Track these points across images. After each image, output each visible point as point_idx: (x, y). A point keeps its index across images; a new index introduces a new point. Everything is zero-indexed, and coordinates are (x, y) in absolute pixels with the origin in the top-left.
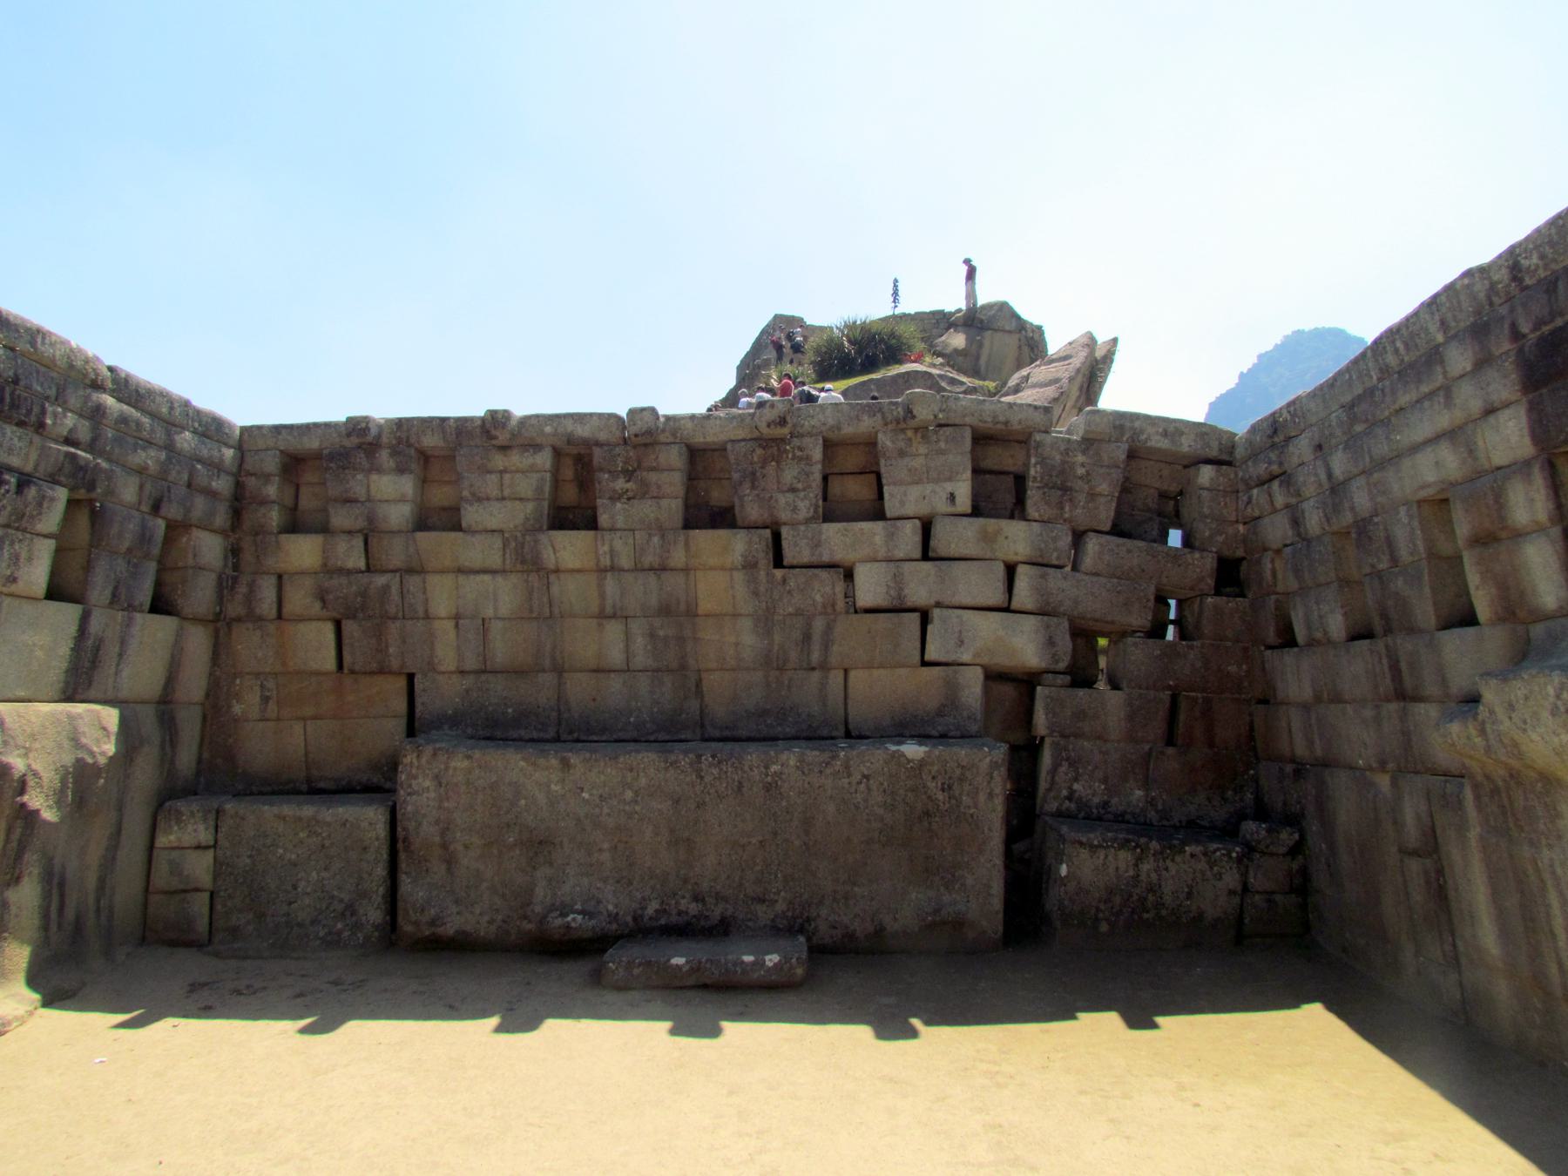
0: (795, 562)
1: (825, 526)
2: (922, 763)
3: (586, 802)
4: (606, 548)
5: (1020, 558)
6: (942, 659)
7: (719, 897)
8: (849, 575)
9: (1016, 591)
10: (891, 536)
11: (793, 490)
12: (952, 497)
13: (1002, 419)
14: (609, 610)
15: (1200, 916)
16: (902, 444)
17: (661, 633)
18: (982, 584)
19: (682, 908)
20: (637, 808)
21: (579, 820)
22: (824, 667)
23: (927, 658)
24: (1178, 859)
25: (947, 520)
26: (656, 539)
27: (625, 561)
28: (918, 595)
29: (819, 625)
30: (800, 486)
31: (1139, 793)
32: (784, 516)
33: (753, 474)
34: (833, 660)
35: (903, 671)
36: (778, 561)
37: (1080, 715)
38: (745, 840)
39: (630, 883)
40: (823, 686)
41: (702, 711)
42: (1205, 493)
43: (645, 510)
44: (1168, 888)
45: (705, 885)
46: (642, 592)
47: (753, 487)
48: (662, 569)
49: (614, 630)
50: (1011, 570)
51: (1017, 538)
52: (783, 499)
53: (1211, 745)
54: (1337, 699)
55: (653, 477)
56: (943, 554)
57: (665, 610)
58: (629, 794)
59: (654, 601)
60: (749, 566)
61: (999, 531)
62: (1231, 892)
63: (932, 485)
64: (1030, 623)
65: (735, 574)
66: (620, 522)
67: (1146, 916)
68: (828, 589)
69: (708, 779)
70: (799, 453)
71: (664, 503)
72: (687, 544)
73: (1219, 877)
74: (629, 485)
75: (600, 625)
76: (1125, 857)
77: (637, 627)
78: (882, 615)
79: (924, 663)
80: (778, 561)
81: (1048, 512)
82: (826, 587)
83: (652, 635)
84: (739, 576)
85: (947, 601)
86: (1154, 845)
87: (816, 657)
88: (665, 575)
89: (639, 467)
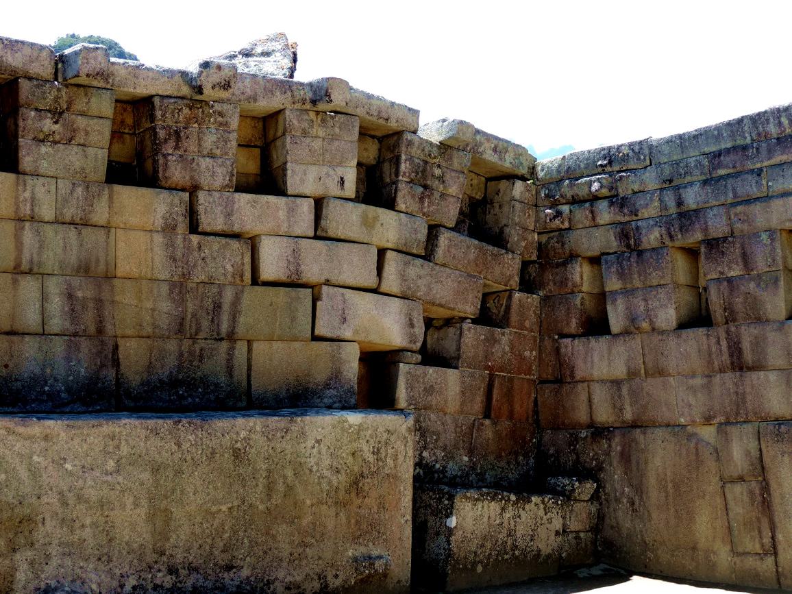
0: (209, 229)
1: (237, 195)
2: (361, 428)
3: (70, 474)
4: (27, 195)
5: (390, 245)
6: (329, 335)
7: (192, 569)
8: (253, 244)
9: (385, 274)
10: (291, 211)
11: (211, 156)
12: (342, 182)
13: (385, 115)
14: (25, 266)
15: (539, 554)
16: (305, 125)
17: (79, 294)
18: (357, 267)
19: (158, 582)
20: (120, 479)
21: (61, 493)
22: (231, 337)
23: (317, 332)
24: (527, 507)
25: (338, 202)
26: (79, 190)
27: (47, 213)
28: (312, 272)
29: (229, 295)
30: (218, 152)
31: (466, 459)
32: (204, 181)
33: (177, 133)
34: (241, 330)
35: (297, 345)
36: (194, 228)
37: (429, 390)
38: (214, 509)
39: (110, 561)
40: (230, 360)
41: (117, 379)
42: (518, 205)
43: (73, 157)
44: (521, 531)
45: (179, 557)
46: (58, 247)
47: (177, 147)
48: (81, 224)
49: (29, 287)
50: (382, 253)
51: (390, 227)
52: (205, 163)
53: (511, 416)
54: (661, 372)
55: (81, 122)
56: (331, 234)
57: (84, 269)
58: (111, 464)
59: (73, 259)
60: (169, 229)
61: (376, 218)
62: (557, 533)
63: (321, 168)
64: (396, 304)
65: (155, 236)
66: (44, 166)
67: (506, 557)
68: (238, 259)
69: (186, 446)
70: (220, 119)
71: (90, 151)
72: (111, 197)
73: (550, 521)
74: (56, 127)
75: (15, 282)
76: (494, 507)
77: (55, 287)
78: (282, 289)
79: (316, 338)
80: (194, 228)
81: (414, 206)
82: (233, 256)
83: (70, 296)
84: (159, 239)
85: (334, 279)
86: (513, 497)
87: (224, 328)
88: (85, 231)
89: (68, 109)
